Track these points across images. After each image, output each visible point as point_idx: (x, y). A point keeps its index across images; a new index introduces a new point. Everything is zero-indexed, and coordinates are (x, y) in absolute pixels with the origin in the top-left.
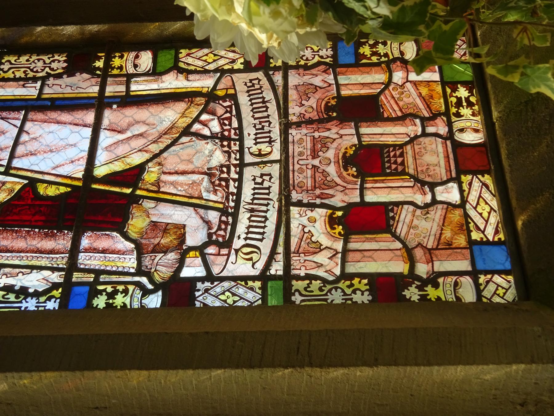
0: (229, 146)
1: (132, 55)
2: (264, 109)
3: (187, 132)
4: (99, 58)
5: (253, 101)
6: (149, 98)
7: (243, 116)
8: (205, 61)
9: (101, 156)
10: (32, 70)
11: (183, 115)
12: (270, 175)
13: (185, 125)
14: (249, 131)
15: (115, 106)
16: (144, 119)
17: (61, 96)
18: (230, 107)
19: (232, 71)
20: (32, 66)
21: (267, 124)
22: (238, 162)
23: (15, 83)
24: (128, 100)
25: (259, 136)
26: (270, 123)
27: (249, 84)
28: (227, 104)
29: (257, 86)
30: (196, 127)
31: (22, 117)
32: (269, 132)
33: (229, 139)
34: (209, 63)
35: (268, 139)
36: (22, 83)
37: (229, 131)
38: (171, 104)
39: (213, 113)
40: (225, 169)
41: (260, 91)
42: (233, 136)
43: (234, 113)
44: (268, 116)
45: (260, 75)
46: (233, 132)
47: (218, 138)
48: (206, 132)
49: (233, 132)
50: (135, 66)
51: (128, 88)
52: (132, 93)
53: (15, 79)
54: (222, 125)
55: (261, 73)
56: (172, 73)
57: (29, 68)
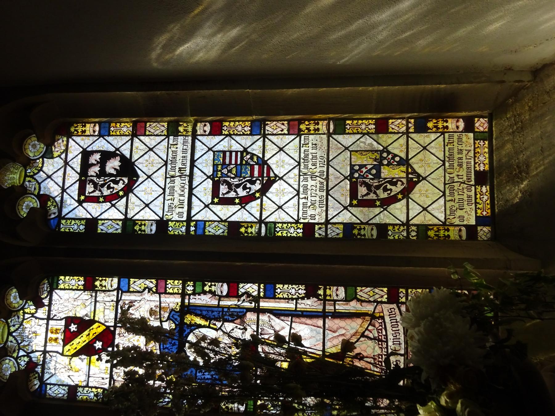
0: (382, 345)
1: (335, 288)
2: (397, 326)
3: (363, 335)
4: (320, 289)
5: (392, 321)
6: (344, 314)
7: (388, 329)
8: (369, 295)
9: (328, 344)
10: (290, 294)
11: (361, 326)
12: (399, 361)
13: (362, 332)
14: (390, 337)
15: (330, 317)
16: (343, 326)
17: (305, 310)
18: (381, 323)
19: (382, 302)
20: (290, 291)
21: (398, 334)
22: (386, 353)
23: (284, 300)
24: (336, 314)
25: (395, 340)
26: (400, 334)
27: (390, 311)
28: (380, 321)
29: (393, 313)
30: (367, 333)
31: (290, 320)
32: (399, 339)
33: (382, 341)
34: (371, 297)
35: (398, 343)
36: (287, 301)
37: (381, 336)
38: (355, 319)
39: (374, 326)
40: (380, 357)
41: (394, 316)
42: (383, 339)
43: (383, 326)
44: (398, 330)
45: (394, 306)
46: (383, 337)
47: (377, 340)
48: (371, 335)
49: (383, 337)
50: (337, 295)
51: (335, 307)
52: (337, 311)
53: (284, 298)
54: (378, 332)
55: (395, 305)
56: (354, 301)
57: (289, 292)
